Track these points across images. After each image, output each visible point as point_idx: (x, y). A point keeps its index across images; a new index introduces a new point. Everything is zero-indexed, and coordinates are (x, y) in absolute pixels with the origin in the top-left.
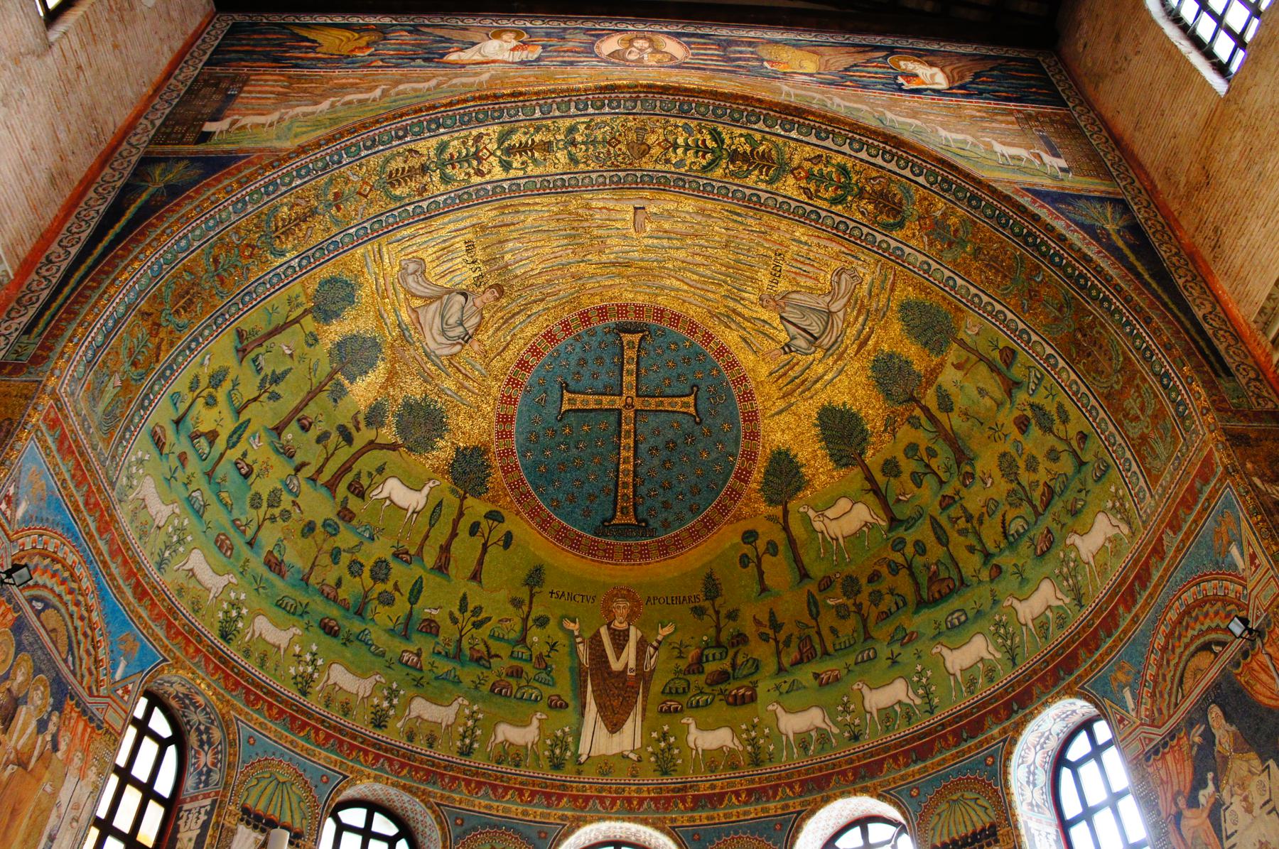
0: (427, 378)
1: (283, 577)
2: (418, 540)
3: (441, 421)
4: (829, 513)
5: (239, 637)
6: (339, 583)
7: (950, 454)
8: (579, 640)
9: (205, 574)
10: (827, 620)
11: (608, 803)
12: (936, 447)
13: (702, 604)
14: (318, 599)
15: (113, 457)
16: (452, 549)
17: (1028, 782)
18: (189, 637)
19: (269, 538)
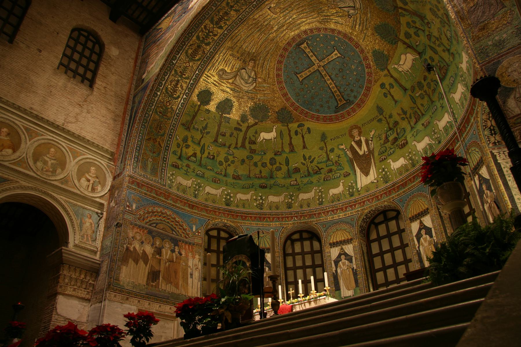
0: (252, 99)
1: (241, 179)
2: (281, 146)
3: (266, 108)
4: (401, 63)
5: (233, 203)
6: (261, 172)
7: (419, 19)
8: (346, 150)
9: (213, 191)
10: (419, 102)
11: (371, 200)
12: (414, 19)
13: (379, 117)
14: (256, 180)
15: (161, 179)
16: (293, 143)
17: (492, 135)
18: (216, 211)
19: (231, 171)
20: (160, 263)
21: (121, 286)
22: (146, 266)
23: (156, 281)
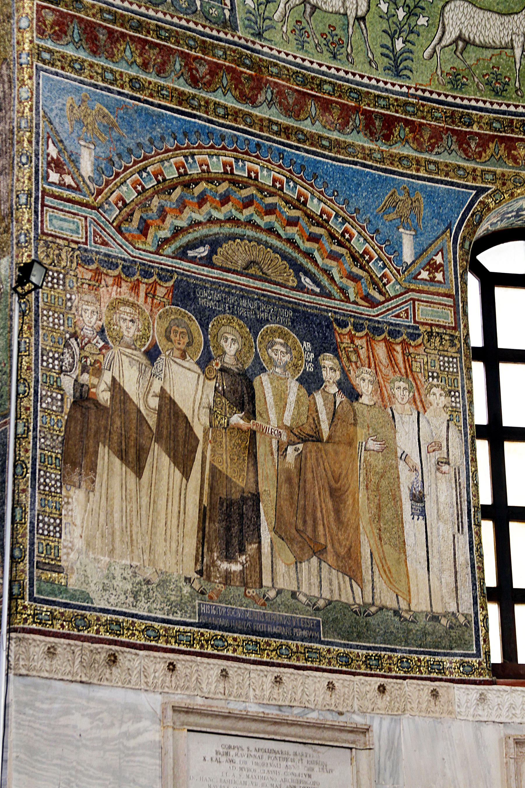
20: (253, 455)
21: (72, 597)
22: (186, 474)
23: (242, 551)
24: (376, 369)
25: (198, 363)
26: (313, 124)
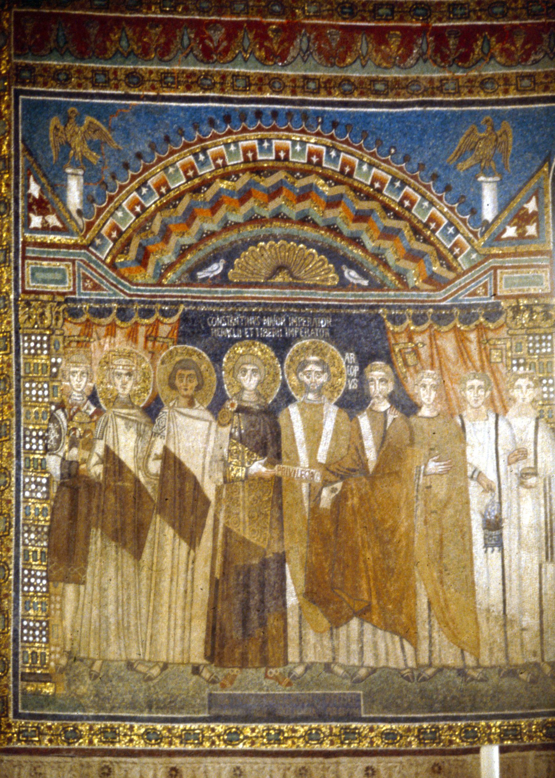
24: (441, 369)
25: (210, 409)
26: (363, 66)
